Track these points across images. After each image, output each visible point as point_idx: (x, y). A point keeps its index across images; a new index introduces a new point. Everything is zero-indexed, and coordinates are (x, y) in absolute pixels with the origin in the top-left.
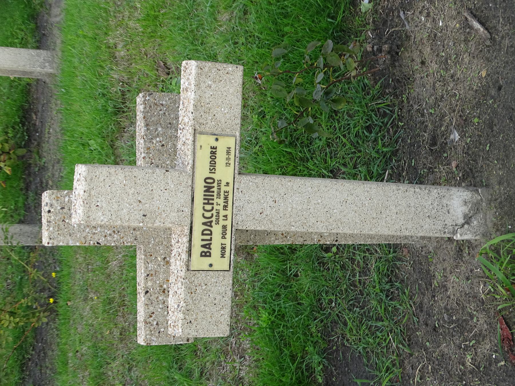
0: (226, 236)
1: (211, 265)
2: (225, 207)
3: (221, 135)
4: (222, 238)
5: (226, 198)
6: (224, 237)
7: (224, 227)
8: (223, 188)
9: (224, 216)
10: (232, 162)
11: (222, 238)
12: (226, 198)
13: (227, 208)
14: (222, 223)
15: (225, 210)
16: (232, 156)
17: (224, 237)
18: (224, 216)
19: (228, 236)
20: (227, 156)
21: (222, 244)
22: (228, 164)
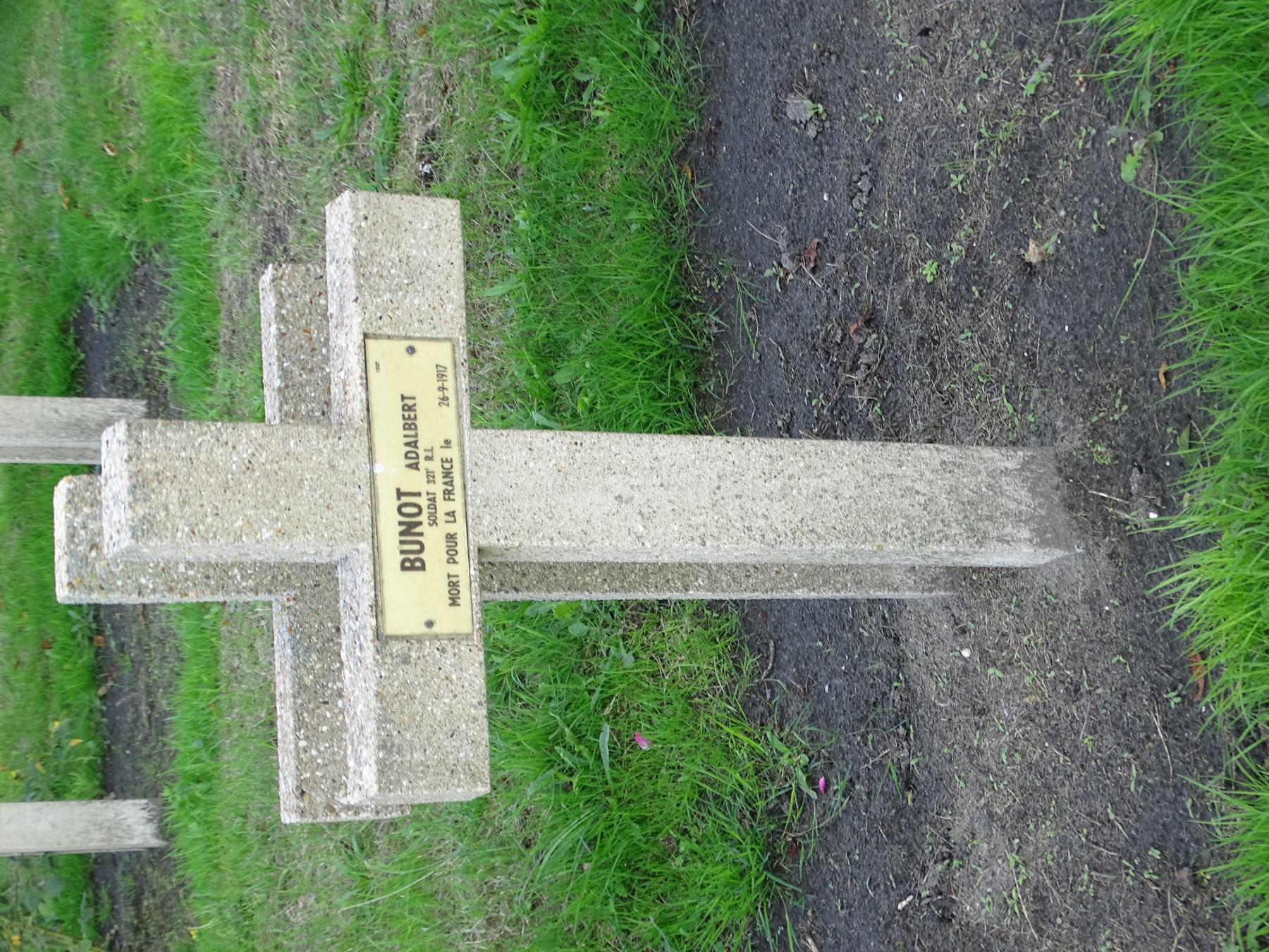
0: (456, 558)
1: (430, 624)
2: (448, 494)
5: (447, 474)
6: (452, 560)
7: (451, 538)
8: (439, 454)
9: (448, 514)
10: (450, 393)
12: (447, 474)
14: (443, 528)
16: (450, 384)
17: (452, 560)
18: (448, 514)
20: (440, 384)
21: (449, 576)
22: (444, 399)
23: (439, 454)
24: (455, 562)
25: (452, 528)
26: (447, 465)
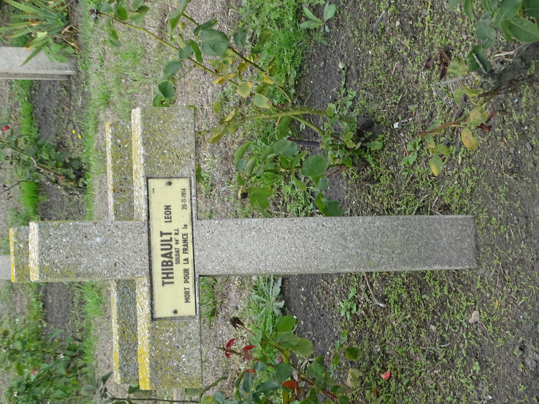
0: (188, 280)
2: (185, 251)
3: (174, 178)
4: (185, 282)
5: (185, 241)
7: (186, 271)
8: (182, 231)
9: (185, 260)
11: (185, 282)
12: (185, 241)
13: (187, 252)
15: (186, 253)
17: (186, 281)
18: (185, 260)
19: (191, 280)
20: (183, 198)
21: (185, 289)
22: (184, 207)
23: (182, 231)
24: (188, 282)
25: (186, 267)
26: (185, 237)
